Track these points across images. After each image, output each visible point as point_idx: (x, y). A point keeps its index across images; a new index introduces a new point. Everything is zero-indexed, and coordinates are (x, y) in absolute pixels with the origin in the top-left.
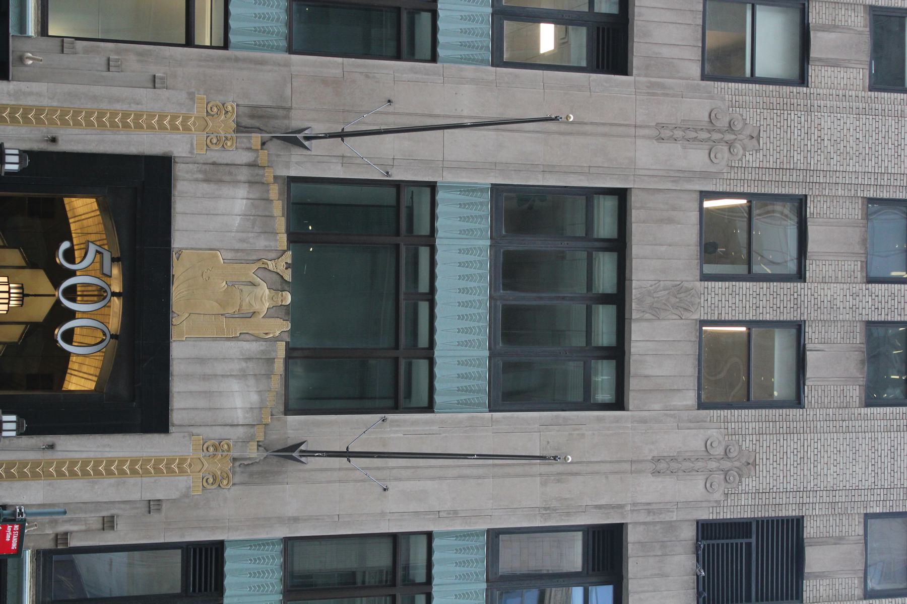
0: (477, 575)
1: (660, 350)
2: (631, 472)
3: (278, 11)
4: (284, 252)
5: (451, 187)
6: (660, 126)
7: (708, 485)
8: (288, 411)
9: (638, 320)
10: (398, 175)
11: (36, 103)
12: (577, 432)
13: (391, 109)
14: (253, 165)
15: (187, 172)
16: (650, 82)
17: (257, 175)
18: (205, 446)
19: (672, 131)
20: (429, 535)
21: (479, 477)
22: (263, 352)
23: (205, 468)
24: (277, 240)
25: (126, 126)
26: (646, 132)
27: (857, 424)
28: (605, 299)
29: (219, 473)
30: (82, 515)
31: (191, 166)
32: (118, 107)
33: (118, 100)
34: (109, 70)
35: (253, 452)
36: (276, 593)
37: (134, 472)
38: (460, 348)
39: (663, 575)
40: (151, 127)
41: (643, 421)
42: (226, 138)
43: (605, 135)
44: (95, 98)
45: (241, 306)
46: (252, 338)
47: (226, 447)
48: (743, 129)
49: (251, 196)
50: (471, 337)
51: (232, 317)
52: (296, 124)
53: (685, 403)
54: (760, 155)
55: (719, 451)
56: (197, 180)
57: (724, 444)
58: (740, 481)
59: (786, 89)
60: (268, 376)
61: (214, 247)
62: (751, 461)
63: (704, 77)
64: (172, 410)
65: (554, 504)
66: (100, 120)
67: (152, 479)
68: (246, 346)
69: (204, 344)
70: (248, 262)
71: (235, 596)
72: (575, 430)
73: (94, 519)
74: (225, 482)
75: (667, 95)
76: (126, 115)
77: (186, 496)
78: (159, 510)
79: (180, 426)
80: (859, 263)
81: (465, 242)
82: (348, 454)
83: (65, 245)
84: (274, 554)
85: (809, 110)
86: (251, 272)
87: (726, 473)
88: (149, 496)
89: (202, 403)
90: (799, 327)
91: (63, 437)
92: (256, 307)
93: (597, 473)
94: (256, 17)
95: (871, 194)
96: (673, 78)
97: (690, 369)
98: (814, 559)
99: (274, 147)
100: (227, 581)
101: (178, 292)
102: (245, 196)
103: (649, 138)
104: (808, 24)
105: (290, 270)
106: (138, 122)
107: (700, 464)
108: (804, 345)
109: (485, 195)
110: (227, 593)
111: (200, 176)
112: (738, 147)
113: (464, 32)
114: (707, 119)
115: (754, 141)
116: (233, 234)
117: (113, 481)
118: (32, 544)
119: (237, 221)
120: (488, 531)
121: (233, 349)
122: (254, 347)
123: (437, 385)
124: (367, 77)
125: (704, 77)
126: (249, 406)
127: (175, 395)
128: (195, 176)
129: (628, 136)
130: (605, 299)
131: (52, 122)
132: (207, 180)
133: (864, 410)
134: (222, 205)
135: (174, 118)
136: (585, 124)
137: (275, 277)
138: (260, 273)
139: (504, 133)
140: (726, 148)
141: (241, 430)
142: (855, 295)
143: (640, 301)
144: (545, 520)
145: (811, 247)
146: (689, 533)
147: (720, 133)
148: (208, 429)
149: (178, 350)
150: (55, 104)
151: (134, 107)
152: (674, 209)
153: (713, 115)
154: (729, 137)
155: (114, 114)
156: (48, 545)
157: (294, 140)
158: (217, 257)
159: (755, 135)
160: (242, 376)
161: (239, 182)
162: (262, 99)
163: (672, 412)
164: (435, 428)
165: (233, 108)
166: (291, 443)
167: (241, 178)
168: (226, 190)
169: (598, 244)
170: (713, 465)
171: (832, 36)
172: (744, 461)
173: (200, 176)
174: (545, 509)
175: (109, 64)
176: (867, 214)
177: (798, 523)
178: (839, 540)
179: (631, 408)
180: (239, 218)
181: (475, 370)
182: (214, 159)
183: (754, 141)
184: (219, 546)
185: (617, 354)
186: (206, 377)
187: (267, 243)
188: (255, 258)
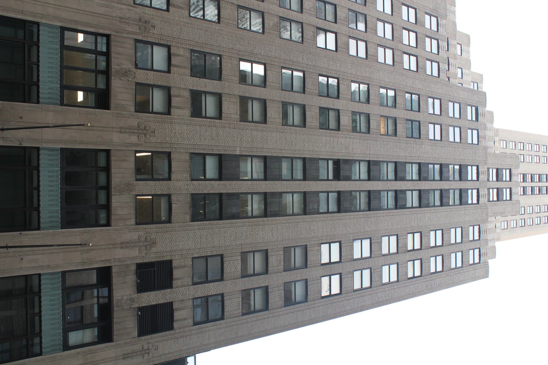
1: (122, 205)
5: (45, 149)
6: (121, 128)
10: (25, 144)
20: (40, 275)
21: (58, 253)
26: (116, 130)
28: (102, 188)
41: (117, 230)
43: (101, 131)
54: (155, 138)
55: (143, 239)
59: (164, 116)
63: (136, 111)
82: (7, 247)
85: (171, 123)
90: (169, 196)
95: (192, 151)
97: (133, 211)
103: (117, 132)
107: (137, 244)
112: (148, 136)
123: (41, 220)
125: (136, 111)
130: (102, 188)
133: (191, 223)
140: (144, 136)
142: (187, 185)
145: (173, 169)
146: (134, 268)
147: (142, 131)
154: (145, 132)
170: (141, 244)
171: (179, 99)
177: (170, 262)
178: (184, 267)
185: (107, 207)
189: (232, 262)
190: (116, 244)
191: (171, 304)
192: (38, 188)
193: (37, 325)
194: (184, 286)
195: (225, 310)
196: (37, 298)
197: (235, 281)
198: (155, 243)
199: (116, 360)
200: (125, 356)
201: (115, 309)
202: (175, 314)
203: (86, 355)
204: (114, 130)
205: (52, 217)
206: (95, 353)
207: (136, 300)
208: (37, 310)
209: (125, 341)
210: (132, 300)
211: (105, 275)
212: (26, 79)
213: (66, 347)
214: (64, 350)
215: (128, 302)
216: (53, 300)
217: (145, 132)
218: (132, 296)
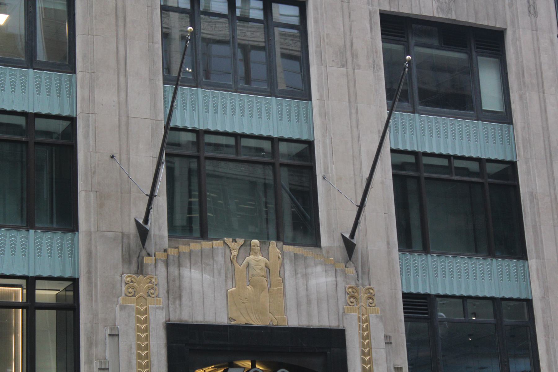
0: (411, 120)
2: (349, 3)
3: (44, 238)
4: (225, 243)
12: (326, 40)
13: (117, 157)
14: (167, 264)
15: (176, 312)
18: (350, 304)
21: (357, 113)
22: (291, 261)
23: (363, 305)
24: (218, 248)
25: (147, 357)
29: (366, 295)
31: (171, 309)
32: (134, 362)
33: (130, 362)
34: (108, 369)
35: (351, 270)
36: (427, 258)
37: (369, 353)
38: (26, 92)
40: (147, 338)
42: (150, 282)
45: (262, 276)
46: (282, 268)
47: (350, 290)
49: (188, 265)
51: (269, 282)
52: (132, 230)
56: (180, 305)
60: (306, 258)
61: (225, 294)
64: (330, 326)
65: (371, 61)
67: (373, 341)
68: (287, 274)
69: (288, 303)
70: (233, 270)
71: (430, 287)
72: (324, 40)
74: (371, 291)
76: (139, 356)
77: (381, 318)
78: (390, 337)
79: (339, 320)
81: (201, 108)
84: (420, 260)
86: (240, 267)
88: (383, 344)
89: (324, 306)
92: (263, 265)
93: (350, 27)
99: (151, 246)
100: (421, 291)
101: (256, 321)
102: (189, 270)
105: (237, 239)
106: (143, 347)
109: (167, 89)
110: (428, 291)
111: (177, 302)
119: (206, 277)
120: (164, 83)
121: (290, 283)
122: (288, 267)
123: (55, 112)
124: (94, 173)
126: (324, 273)
127: (321, 324)
128: (178, 306)
132: (180, 297)
134: (196, 287)
135: (139, 321)
136: (116, 5)
137: (242, 250)
138: (240, 262)
139: (128, 71)
144: (380, 68)
148: (340, 302)
151: (134, 350)
157: (143, 233)
158: (232, 292)
160: (306, 276)
161: (179, 274)
162: (117, 254)
164: (328, 141)
165: (129, 277)
166: (342, 244)
167: (189, 273)
168: (186, 283)
169: (196, 7)
173: (177, 302)
174: (374, 68)
175: (103, 369)
180: (204, 275)
181: (284, 108)
182: (165, 292)
186: (309, 302)
188: (230, 265)
193: (223, 140)
196: (209, 139)
199: (537, 31)
200: (532, 11)
201: (454, 17)
203: (524, 83)
205: (60, 89)
206: (522, 67)
208: (267, 145)
209: (507, 7)
212: (23, 139)
213: (505, 117)
214: (309, 98)
216: (216, 107)
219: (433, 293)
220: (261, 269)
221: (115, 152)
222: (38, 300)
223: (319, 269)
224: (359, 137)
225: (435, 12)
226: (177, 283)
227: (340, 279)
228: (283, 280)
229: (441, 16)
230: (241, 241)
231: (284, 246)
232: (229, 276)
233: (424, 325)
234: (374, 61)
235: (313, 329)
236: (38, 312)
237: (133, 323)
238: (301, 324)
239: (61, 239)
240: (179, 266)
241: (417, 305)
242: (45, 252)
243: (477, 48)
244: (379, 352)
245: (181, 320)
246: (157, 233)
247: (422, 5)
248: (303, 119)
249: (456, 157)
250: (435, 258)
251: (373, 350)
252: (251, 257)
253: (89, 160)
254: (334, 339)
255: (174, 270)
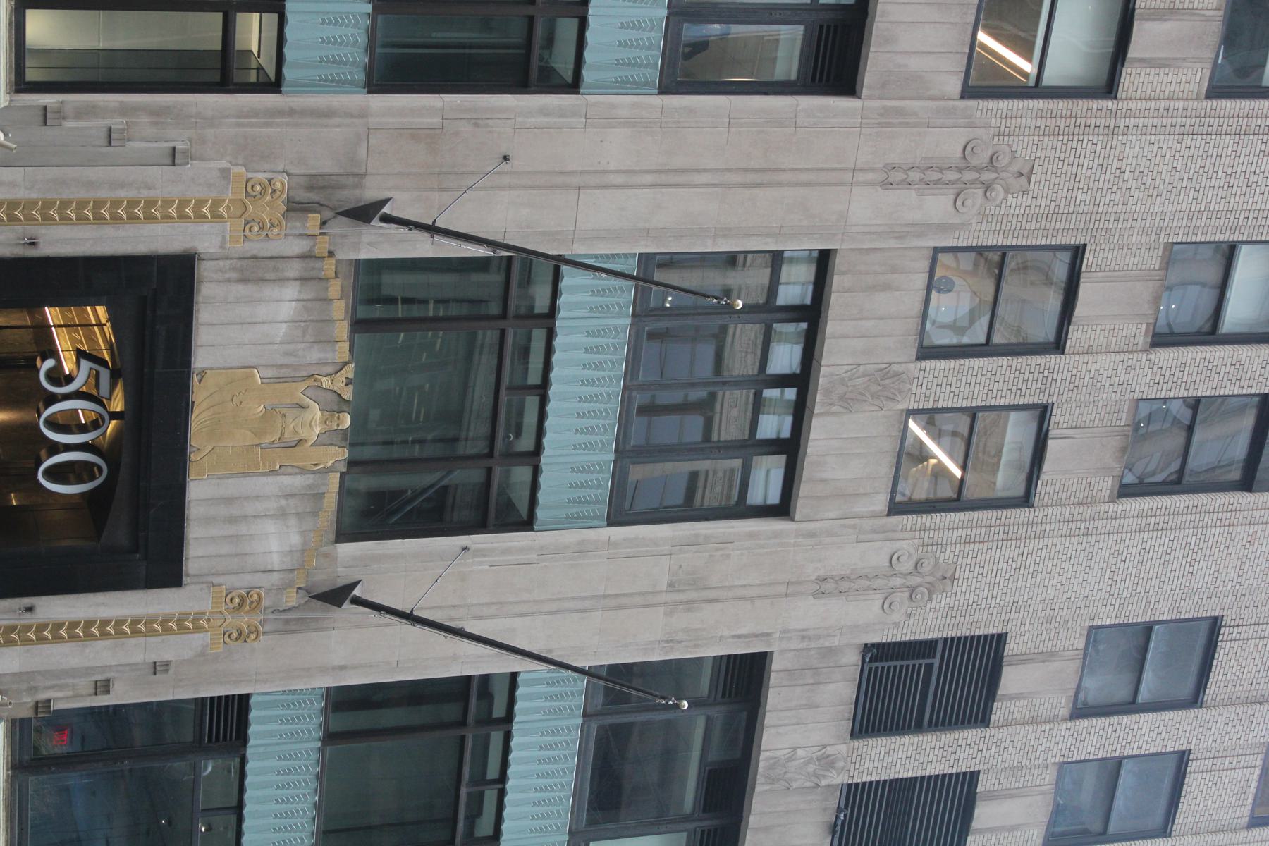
1: (845, 447)
2: (786, 595)
3: (356, 31)
4: (345, 364)
7: (886, 606)
8: (343, 535)
9: (821, 414)
11: (9, 196)
12: (719, 553)
13: (505, 167)
16: (884, 108)
17: (313, 269)
19: (905, 171)
21: (585, 610)
22: (310, 487)
25: (133, 218)
26: (870, 176)
27: (1100, 524)
28: (782, 381)
30: (70, 681)
31: (221, 263)
32: (122, 194)
33: (122, 186)
34: (110, 144)
35: (292, 598)
36: (314, 740)
39: (811, 706)
41: (812, 534)
42: (272, 225)
43: (808, 184)
44: (90, 184)
45: (282, 434)
47: (255, 597)
48: (1010, 164)
49: (303, 296)
50: (592, 438)
51: (271, 447)
52: (371, 194)
53: (872, 508)
54: (1028, 199)
55: (907, 566)
56: (229, 280)
57: (915, 558)
58: (930, 599)
59: (1082, 105)
60: (315, 514)
62: (949, 575)
66: (98, 212)
67: (159, 639)
68: (286, 480)
69: (230, 481)
70: (294, 380)
72: (717, 550)
73: (85, 684)
74: (253, 636)
75: (907, 125)
76: (133, 204)
77: (203, 654)
78: (167, 671)
80: (1144, 326)
83: (50, 363)
86: (299, 392)
87: (912, 590)
88: (153, 657)
89: (225, 549)
90: (1043, 413)
91: (44, 598)
92: (303, 435)
94: (323, 42)
96: (919, 99)
98: (1011, 679)
99: (341, 227)
100: (253, 729)
101: (198, 421)
102: (295, 297)
103: (872, 184)
104: (1134, 9)
105: (351, 387)
106: (150, 211)
107: (879, 582)
108: (1047, 431)
109: (631, 261)
110: (251, 742)
111: (234, 275)
112: (998, 192)
113: (623, 45)
114: (959, 154)
115: (1023, 180)
116: (276, 347)
117: (108, 643)
118: (6, 714)
119: (282, 329)
121: (270, 485)
122: (297, 482)
123: (588, 55)
124: (476, 125)
127: (191, 542)
128: (227, 276)
129: (842, 184)
130: (782, 381)
131: (30, 219)
132: (244, 281)
137: (331, 396)
138: (310, 392)
140: (980, 192)
141: (276, 576)
143: (828, 392)
144: (666, 653)
145: (1080, 310)
146: (853, 658)
147: (977, 172)
149: (198, 491)
150: (34, 196)
151: (145, 194)
152: (894, 270)
153: (969, 149)
154: (987, 176)
155: (116, 203)
156: (26, 713)
157: (364, 213)
158: (254, 376)
159: (1025, 171)
160: (282, 515)
161: (288, 279)
162: (325, 165)
163: (851, 522)
164: (534, 556)
165: (283, 186)
166: (341, 582)
167: (288, 297)
168: (269, 291)
169: (779, 315)
170: (897, 582)
172: (939, 575)
173: (234, 275)
174: (668, 642)
175: (110, 136)
176: (1168, 263)
178: (1051, 656)
179: (797, 517)
180: (284, 325)
182: (254, 252)
183: (1023, 180)
184: (244, 700)
185: (790, 448)
186: (232, 520)
187: (322, 355)
188: (304, 374)
189: (1252, 643)
190: (799, 583)
191: (974, 776)
192: (542, 389)
194: (1035, 721)
195: (1183, 806)
196: (539, 335)
197: (1249, 710)
198: (953, 578)
202: (977, 811)
204: (860, 177)
205: (631, 64)
207: (840, 764)
210: (828, 762)
211: (744, 678)
214: (611, 523)
215: (811, 768)
216: (597, 350)
217: (987, 176)
218: (830, 750)
219: (249, 751)
220: (296, 432)
221: (515, 164)
222: (241, 17)
223: (295, 539)
224: (540, 613)
225: (767, 754)
226: (271, 275)
227: (275, 578)
228: (274, 473)
229: (761, 764)
230: (348, 394)
231: (338, 475)
232: (284, 372)
233: (188, 735)
234: (679, 642)
235: (183, 527)
236: (219, 16)
237: (196, 192)
238: (192, 505)
239: (355, 62)
240: (303, 280)
241: (226, 721)
242: (329, 32)
243: (703, 832)
244: (138, 651)
245: (200, 282)
246: (365, 239)
247: (781, 730)
248: (574, 510)
249: (502, 794)
250: (315, 756)
251: (142, 640)
252: (319, 413)
253: (499, 116)
254: (164, 567)
255: (294, 269)
